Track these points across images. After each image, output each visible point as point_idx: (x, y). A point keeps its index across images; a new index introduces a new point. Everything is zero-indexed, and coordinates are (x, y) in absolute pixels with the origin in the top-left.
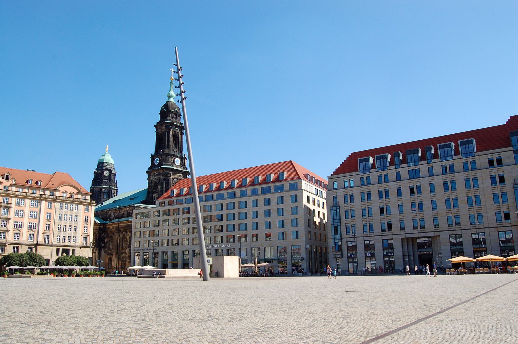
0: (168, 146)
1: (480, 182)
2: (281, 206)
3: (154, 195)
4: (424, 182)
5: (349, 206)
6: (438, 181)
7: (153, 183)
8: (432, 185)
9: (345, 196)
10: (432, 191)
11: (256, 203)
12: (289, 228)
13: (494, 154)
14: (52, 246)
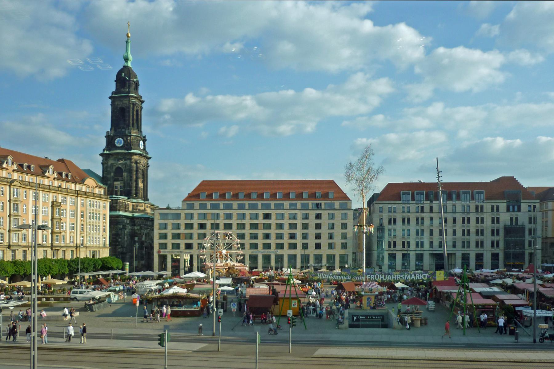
0: (133, 126)
1: (485, 220)
2: (332, 221)
3: (116, 183)
7: (114, 169)
12: (338, 241)
13: (495, 203)
14: (86, 247)
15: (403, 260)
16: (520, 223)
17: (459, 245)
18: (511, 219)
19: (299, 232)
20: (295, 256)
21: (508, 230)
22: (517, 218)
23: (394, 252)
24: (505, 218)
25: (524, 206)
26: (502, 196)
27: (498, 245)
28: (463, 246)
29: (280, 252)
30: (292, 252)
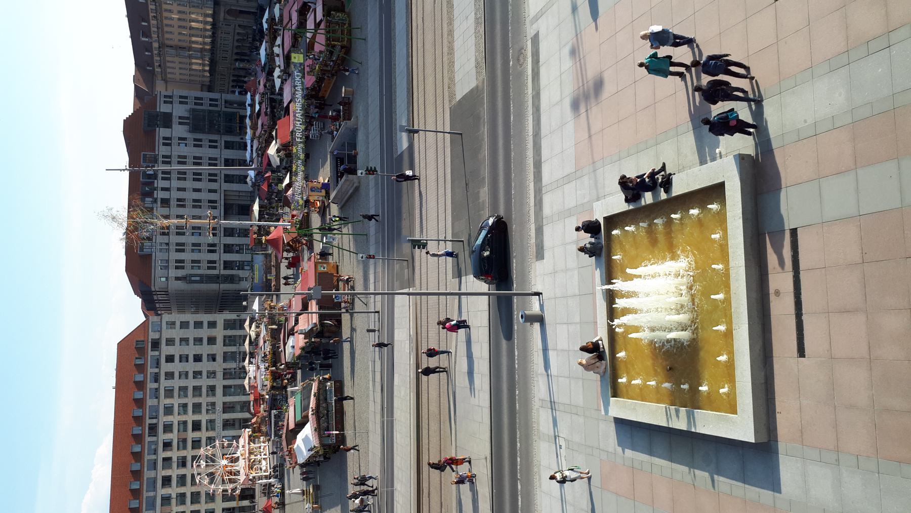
4: (175, 195)
5: (188, 265)
6: (175, 184)
8: (179, 189)
9: (177, 268)
10: (184, 190)
11: (170, 375)
12: (204, 333)
13: (159, 141)
15: (232, 253)
16: (186, 115)
17: (214, 186)
18: (180, 123)
19: (191, 383)
20: (225, 387)
21: (195, 129)
22: (180, 118)
23: (222, 262)
24: (179, 130)
25: (164, 108)
26: (150, 134)
27: (216, 141)
28: (215, 181)
29: (219, 407)
30: (219, 391)
